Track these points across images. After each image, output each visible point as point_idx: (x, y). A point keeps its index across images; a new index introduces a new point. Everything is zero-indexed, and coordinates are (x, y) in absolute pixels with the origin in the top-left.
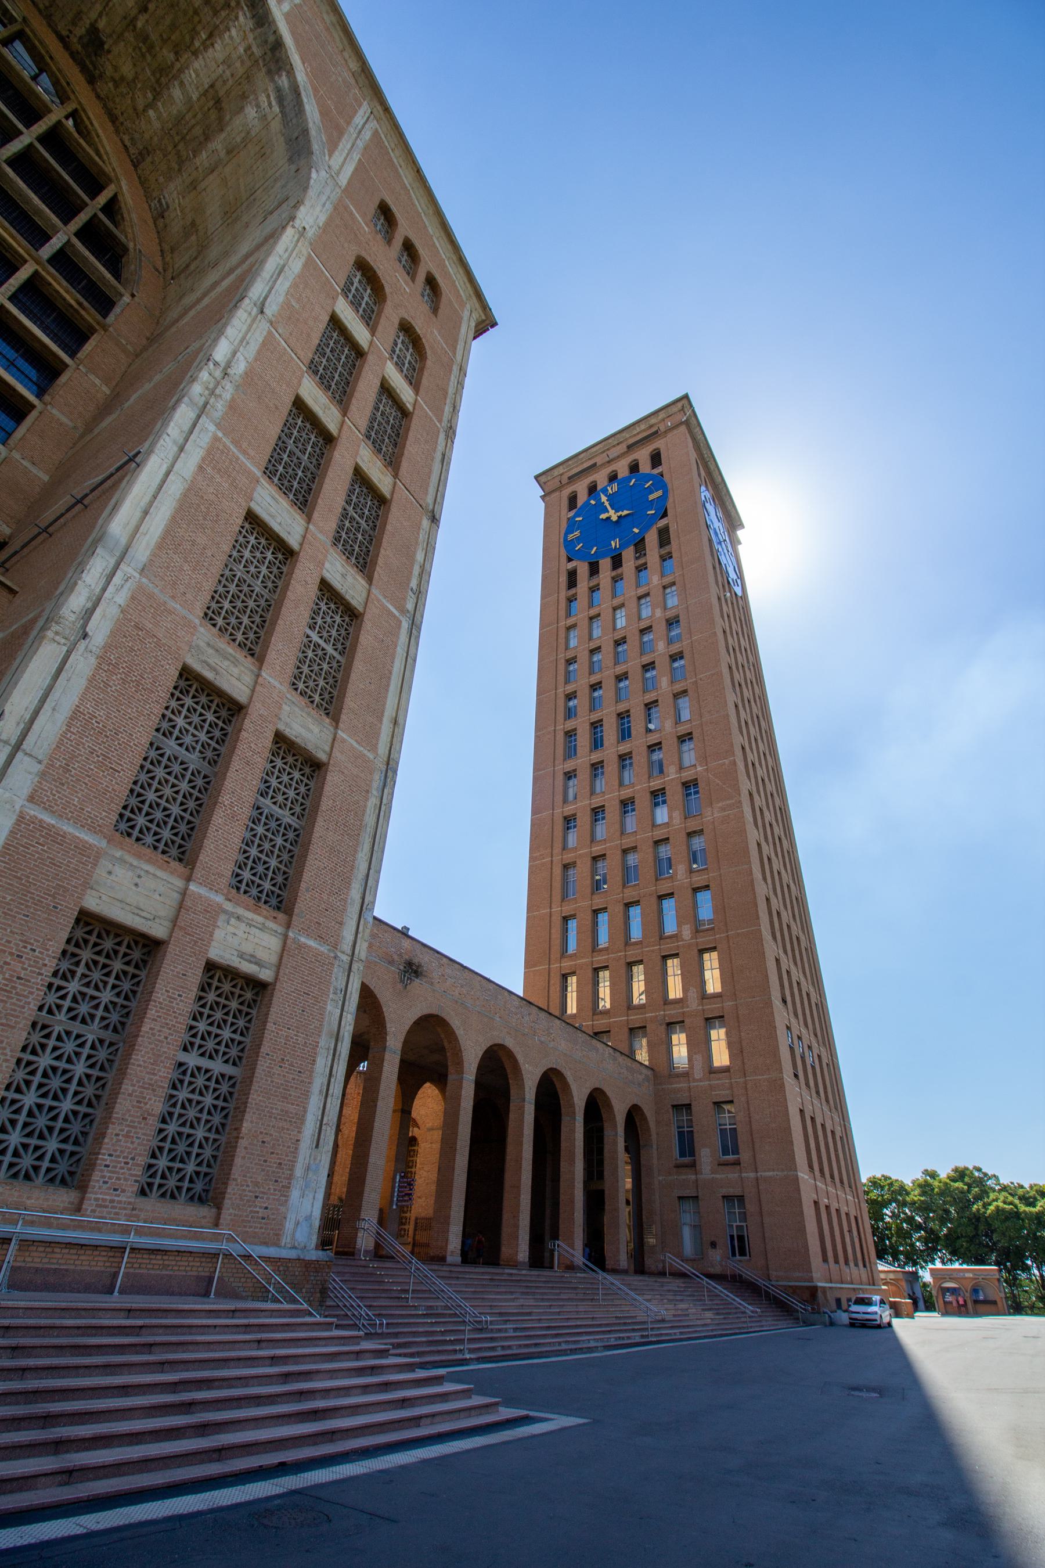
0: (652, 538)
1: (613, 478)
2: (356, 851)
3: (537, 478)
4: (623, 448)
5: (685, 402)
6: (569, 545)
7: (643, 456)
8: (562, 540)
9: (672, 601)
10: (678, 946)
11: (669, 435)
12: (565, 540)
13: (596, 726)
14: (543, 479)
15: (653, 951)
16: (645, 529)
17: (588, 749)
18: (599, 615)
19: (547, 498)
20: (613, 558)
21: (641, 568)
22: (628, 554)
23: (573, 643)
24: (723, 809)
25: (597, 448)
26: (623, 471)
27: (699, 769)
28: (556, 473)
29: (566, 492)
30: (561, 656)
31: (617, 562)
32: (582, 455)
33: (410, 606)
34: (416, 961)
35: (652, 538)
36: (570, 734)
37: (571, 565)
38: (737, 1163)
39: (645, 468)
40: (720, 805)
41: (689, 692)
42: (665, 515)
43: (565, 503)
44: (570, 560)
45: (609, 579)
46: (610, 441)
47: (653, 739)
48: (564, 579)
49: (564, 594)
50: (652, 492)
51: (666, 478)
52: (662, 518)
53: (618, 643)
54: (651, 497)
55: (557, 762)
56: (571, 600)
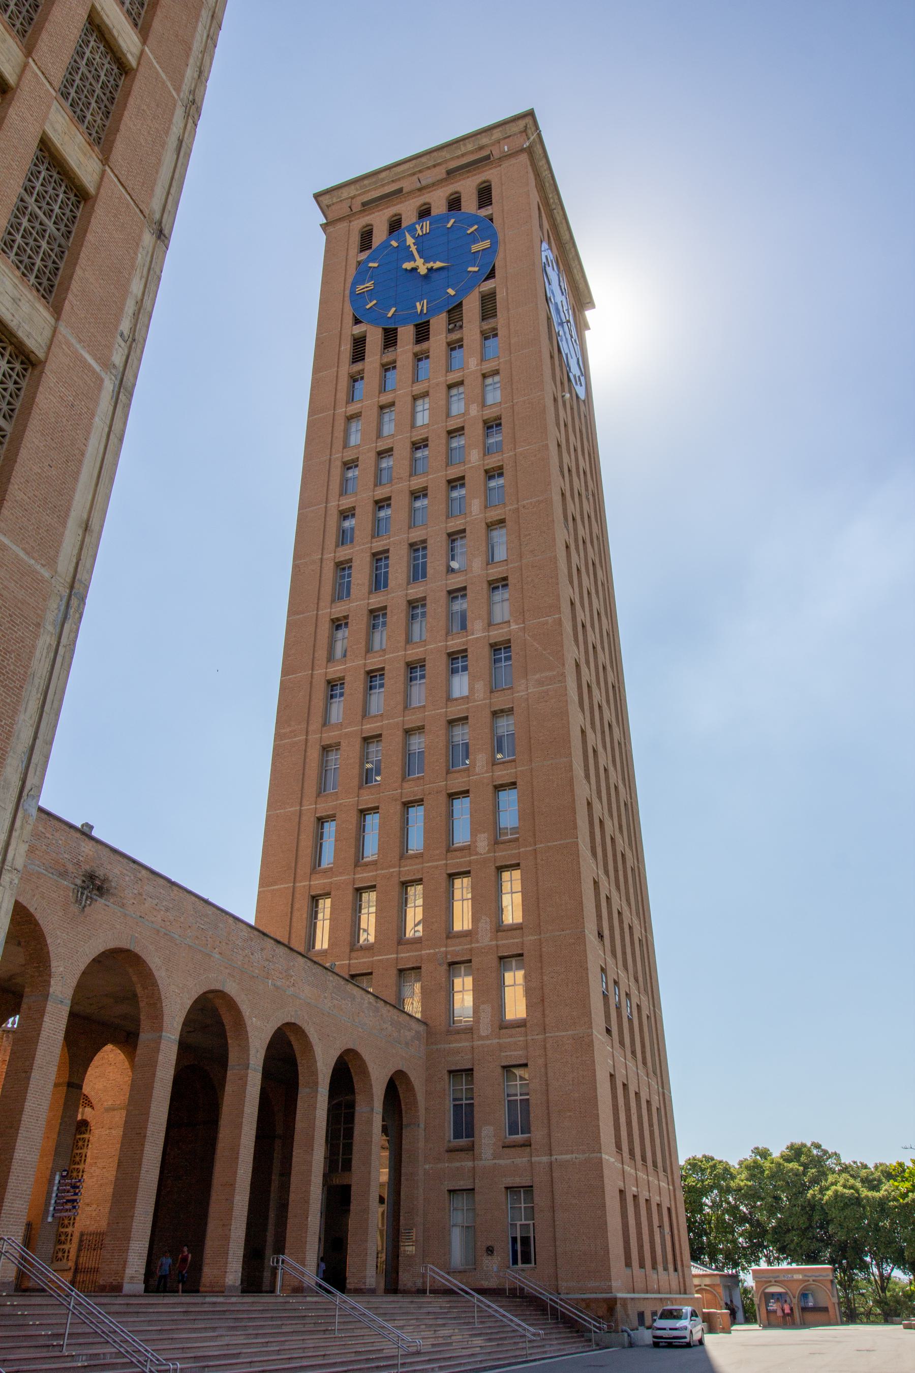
0: (472, 306)
1: (424, 213)
2: (15, 711)
3: (317, 196)
4: (440, 172)
5: (528, 120)
6: (356, 299)
7: (468, 187)
8: (347, 292)
9: (494, 396)
10: (470, 862)
11: (505, 164)
12: (352, 292)
13: (379, 557)
14: (326, 200)
15: (436, 867)
16: (465, 291)
17: (365, 589)
18: (392, 404)
19: (331, 229)
20: (416, 326)
21: (454, 346)
22: (439, 323)
23: (355, 439)
24: (540, 683)
25: (405, 166)
26: (439, 207)
27: (514, 627)
28: (345, 193)
29: (358, 224)
30: (337, 456)
31: (422, 333)
32: (383, 175)
33: (118, 359)
34: (100, 873)
35: (472, 306)
36: (343, 566)
37: (358, 330)
38: (527, 1144)
39: (469, 205)
40: (537, 676)
41: (508, 523)
42: (491, 275)
43: (355, 239)
44: (357, 321)
45: (410, 356)
46: (424, 160)
47: (455, 582)
48: (347, 348)
49: (346, 368)
50: (475, 241)
51: (497, 224)
52: (487, 279)
54: (475, 248)
55: (322, 604)
56: (355, 379)
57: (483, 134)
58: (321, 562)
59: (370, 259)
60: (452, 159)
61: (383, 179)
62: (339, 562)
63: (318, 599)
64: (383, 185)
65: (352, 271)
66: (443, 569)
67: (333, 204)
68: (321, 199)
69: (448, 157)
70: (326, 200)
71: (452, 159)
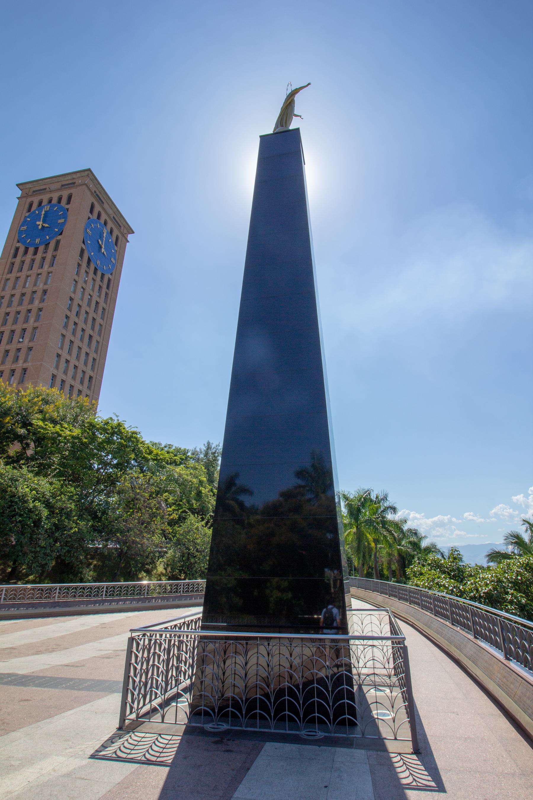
1: (50, 201)
4: (58, 186)
6: (20, 232)
7: (65, 194)
8: (18, 228)
12: (20, 229)
18: (20, 277)
22: (41, 248)
29: (29, 200)
32: (40, 182)
37: (18, 245)
42: (61, 234)
43: (27, 206)
44: (18, 242)
46: (54, 179)
47: (20, 346)
48: (13, 251)
50: (60, 219)
52: (59, 235)
53: (23, 295)
59: (28, 217)
64: (41, 186)
66: (17, 341)
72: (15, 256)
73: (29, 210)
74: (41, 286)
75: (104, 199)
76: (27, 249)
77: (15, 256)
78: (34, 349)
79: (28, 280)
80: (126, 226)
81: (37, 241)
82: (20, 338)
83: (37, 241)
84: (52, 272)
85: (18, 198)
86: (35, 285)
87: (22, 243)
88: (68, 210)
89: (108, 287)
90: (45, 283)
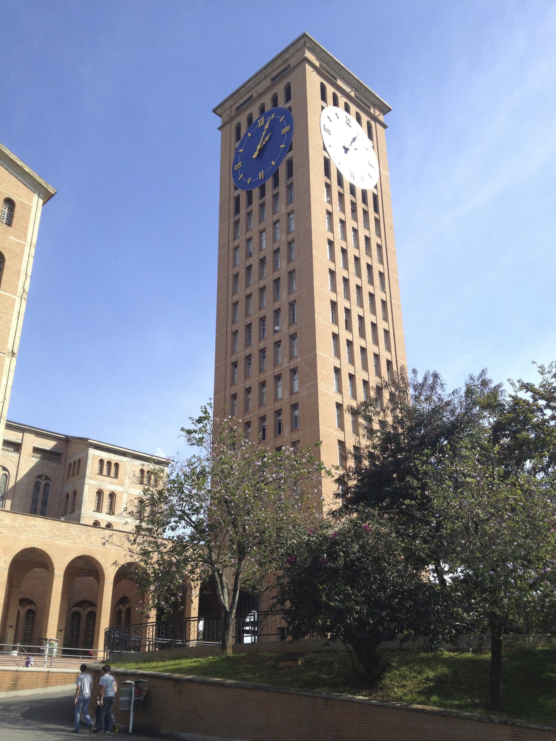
1: (262, 110)
3: (214, 111)
4: (267, 82)
5: (305, 38)
6: (235, 174)
7: (280, 90)
12: (233, 169)
16: (278, 163)
19: (223, 130)
22: (269, 183)
25: (251, 82)
28: (227, 105)
37: (236, 193)
42: (291, 149)
43: (234, 134)
44: (236, 189)
46: (259, 76)
47: (277, 338)
48: (232, 205)
55: (227, 356)
56: (237, 223)
57: (285, 53)
58: (226, 334)
60: (273, 71)
61: (243, 92)
62: (235, 332)
63: (226, 354)
64: (244, 96)
65: (233, 156)
66: (272, 331)
67: (223, 112)
68: (217, 111)
69: (271, 70)
70: (219, 111)
71: (273, 71)
72: (237, 211)
73: (238, 138)
74: (282, 237)
75: (335, 72)
76: (250, 194)
77: (237, 211)
78: (298, 334)
79: (264, 238)
80: (377, 102)
81: (261, 175)
82: (275, 325)
83: (261, 175)
84: (292, 212)
85: (220, 129)
86: (274, 241)
87: (243, 188)
88: (290, 109)
89: (376, 210)
90: (288, 232)
